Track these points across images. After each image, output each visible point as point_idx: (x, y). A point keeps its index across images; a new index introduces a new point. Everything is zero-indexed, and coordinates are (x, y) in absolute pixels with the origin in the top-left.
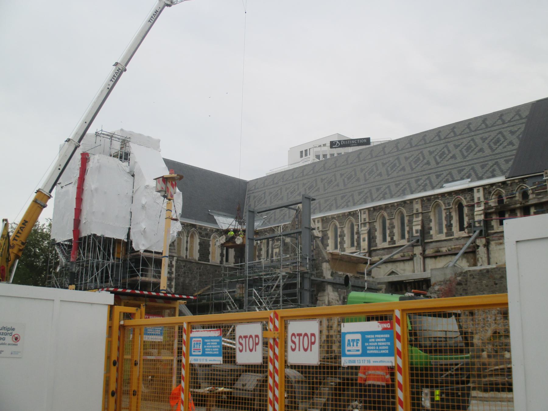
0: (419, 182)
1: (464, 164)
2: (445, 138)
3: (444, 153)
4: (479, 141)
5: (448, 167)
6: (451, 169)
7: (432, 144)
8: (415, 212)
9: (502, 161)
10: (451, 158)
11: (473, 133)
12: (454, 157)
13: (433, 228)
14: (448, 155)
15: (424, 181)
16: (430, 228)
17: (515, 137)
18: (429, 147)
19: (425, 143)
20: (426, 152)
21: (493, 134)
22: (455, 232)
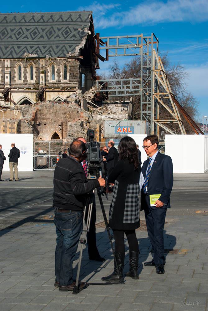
0: (7, 49)
1: (33, 43)
2: (19, 22)
3: (20, 33)
4: (40, 31)
5: (24, 43)
6: (26, 45)
7: (12, 24)
8: (6, 66)
9: (54, 46)
10: (25, 37)
11: (36, 24)
12: (26, 37)
13: (16, 77)
14: (23, 35)
15: (11, 49)
16: (15, 77)
17: (60, 32)
18: (10, 26)
19: (7, 23)
20: (8, 29)
21: (49, 27)
22: (28, 80)
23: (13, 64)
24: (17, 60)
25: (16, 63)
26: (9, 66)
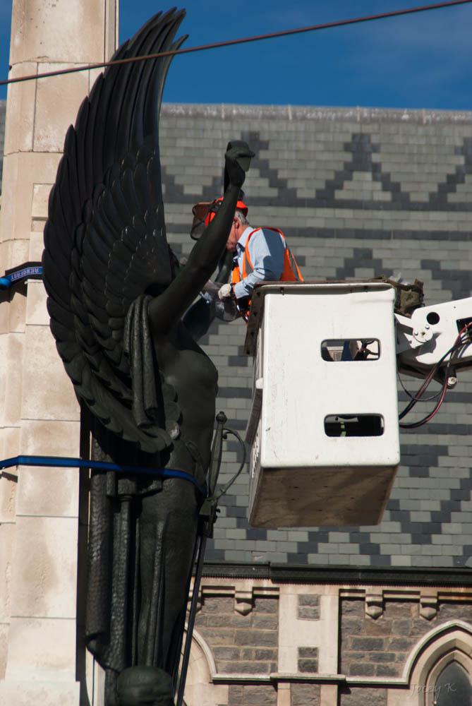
23: (370, 645)
24: (429, 593)
25: (415, 634)
26: (327, 667)
